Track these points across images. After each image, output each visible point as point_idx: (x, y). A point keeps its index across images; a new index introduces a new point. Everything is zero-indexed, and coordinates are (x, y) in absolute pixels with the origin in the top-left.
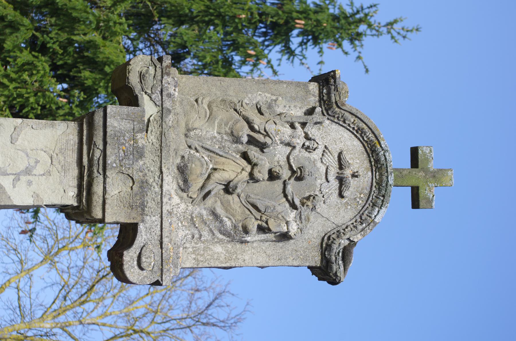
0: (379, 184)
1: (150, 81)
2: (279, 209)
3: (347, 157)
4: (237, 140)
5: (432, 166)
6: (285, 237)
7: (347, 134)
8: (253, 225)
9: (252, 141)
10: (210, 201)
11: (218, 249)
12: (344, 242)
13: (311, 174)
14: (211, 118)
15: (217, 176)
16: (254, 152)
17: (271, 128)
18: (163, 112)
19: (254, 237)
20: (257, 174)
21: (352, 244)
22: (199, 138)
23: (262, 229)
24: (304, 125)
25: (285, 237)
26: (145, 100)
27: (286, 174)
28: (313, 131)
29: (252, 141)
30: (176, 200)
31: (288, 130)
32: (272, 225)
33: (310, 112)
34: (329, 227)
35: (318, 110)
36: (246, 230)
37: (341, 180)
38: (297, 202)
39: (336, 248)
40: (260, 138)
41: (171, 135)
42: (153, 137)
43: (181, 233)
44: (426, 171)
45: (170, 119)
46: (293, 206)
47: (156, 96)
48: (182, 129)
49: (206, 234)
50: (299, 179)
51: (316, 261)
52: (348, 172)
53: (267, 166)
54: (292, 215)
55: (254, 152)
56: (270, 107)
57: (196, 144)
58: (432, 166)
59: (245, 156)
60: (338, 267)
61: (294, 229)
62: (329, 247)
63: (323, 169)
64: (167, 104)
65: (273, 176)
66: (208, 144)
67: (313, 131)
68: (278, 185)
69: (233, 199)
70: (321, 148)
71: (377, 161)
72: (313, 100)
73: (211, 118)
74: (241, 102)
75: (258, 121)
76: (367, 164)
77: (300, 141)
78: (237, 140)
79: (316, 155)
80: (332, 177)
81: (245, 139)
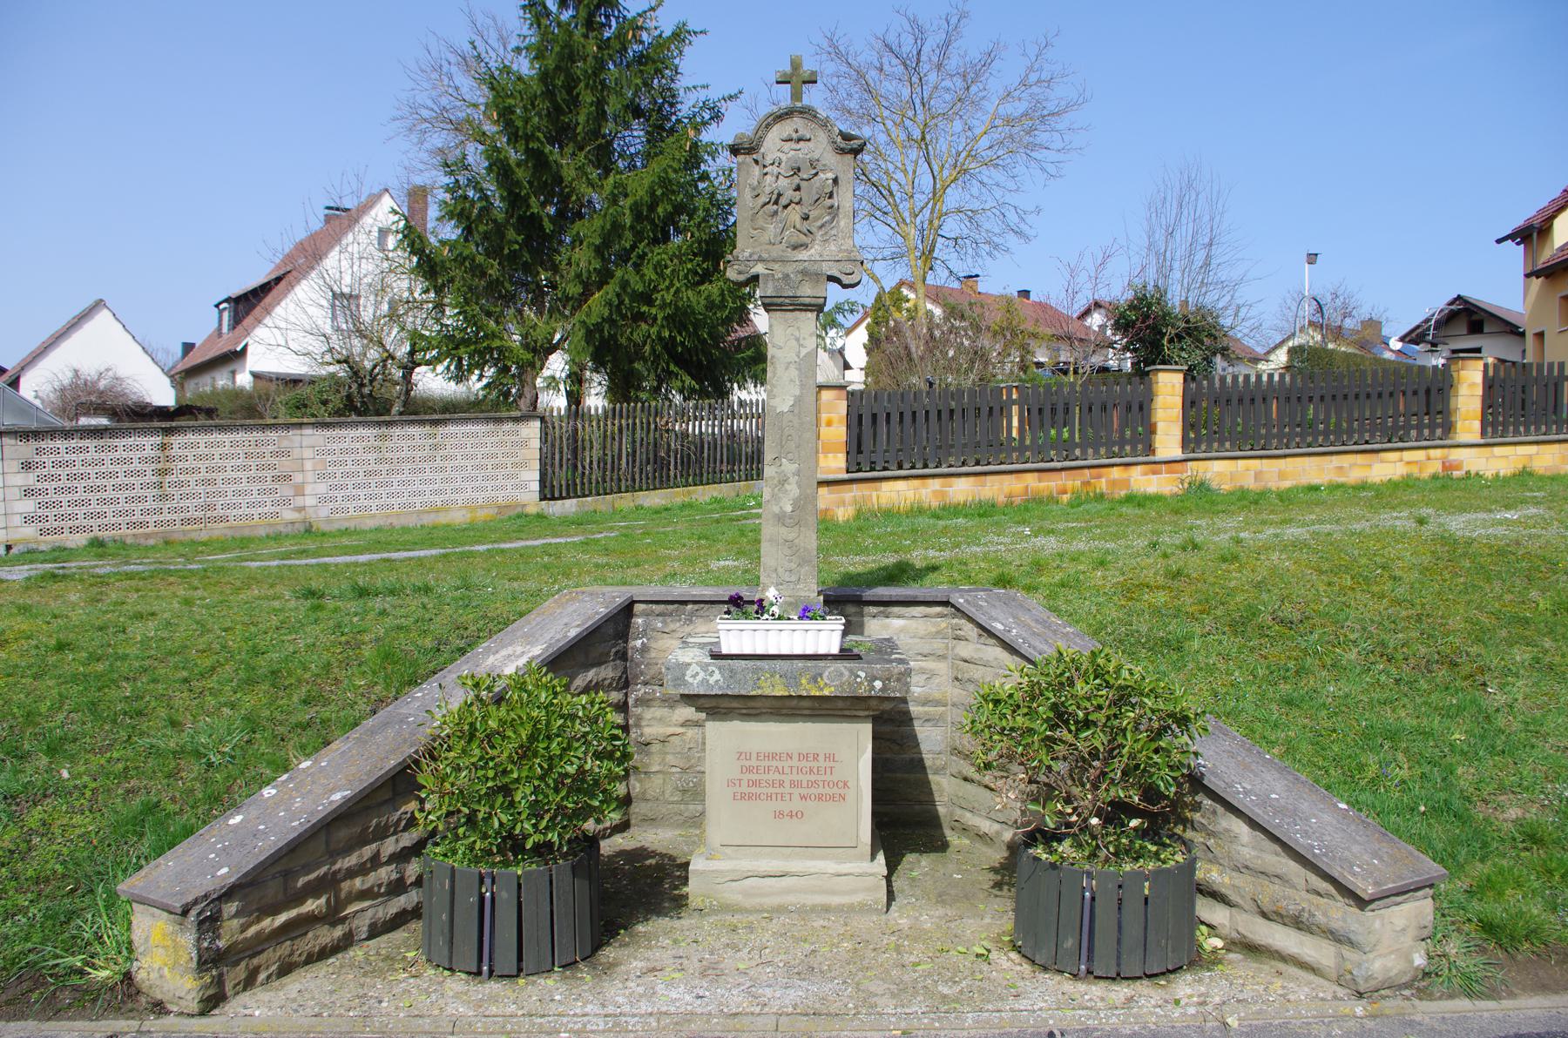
0: (801, 113)
1: (742, 268)
2: (818, 184)
3: (785, 136)
4: (776, 213)
5: (788, 69)
6: (835, 181)
7: (770, 135)
8: (828, 202)
9: (776, 203)
10: (813, 230)
11: (842, 223)
12: (839, 139)
13: (796, 162)
14: (763, 229)
15: (798, 226)
16: (783, 201)
17: (768, 190)
18: (761, 260)
19: (835, 202)
20: (796, 200)
21: (841, 133)
22: (775, 236)
23: (831, 196)
24: (765, 166)
25: (835, 181)
26: (754, 271)
27: (796, 180)
28: (768, 161)
29: (776, 203)
30: (813, 251)
31: (768, 177)
32: (828, 190)
33: (756, 162)
34: (829, 148)
35: (755, 156)
36: (831, 207)
37: (800, 140)
38: (814, 171)
39: (843, 144)
40: (774, 197)
41: (774, 254)
42: (776, 266)
43: (833, 248)
44: (792, 75)
45: (765, 256)
46: (816, 174)
47: (751, 264)
48: (770, 247)
49: (833, 232)
50: (799, 170)
51: (850, 157)
52: (795, 136)
53: (791, 192)
54: (821, 175)
55: (783, 201)
56: (754, 189)
57: (779, 239)
58: (788, 69)
59: (785, 207)
60: (855, 144)
61: (831, 175)
62: (842, 149)
63: (792, 153)
64: (756, 257)
65: (798, 189)
66: (779, 231)
67: (768, 161)
68: (803, 184)
69: (812, 215)
70: (779, 154)
71: (787, 114)
72: (749, 159)
73: (763, 229)
74: (752, 209)
75: (764, 199)
76: (788, 121)
77: (775, 169)
78: (776, 213)
79: (784, 158)
80: (798, 146)
81: (775, 207)
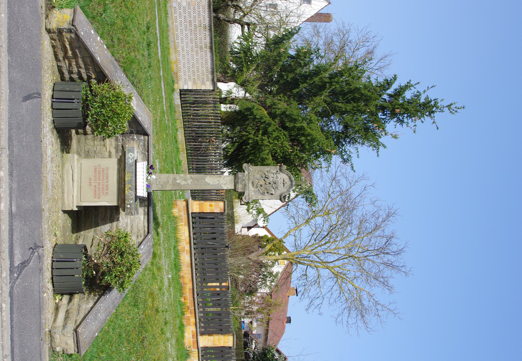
1: (247, 168)
3: (285, 180)
6: (272, 194)
7: (285, 175)
8: (266, 192)
9: (265, 177)
10: (258, 188)
11: (260, 196)
12: (284, 195)
16: (266, 179)
17: (269, 175)
18: (249, 173)
19: (266, 194)
23: (268, 193)
26: (246, 171)
28: (277, 175)
29: (265, 177)
31: (273, 175)
32: (269, 192)
33: (277, 172)
37: (284, 184)
39: (282, 196)
40: (267, 177)
41: (251, 177)
42: (247, 177)
45: (250, 174)
49: (257, 194)
52: (285, 182)
54: (273, 190)
56: (269, 171)
59: (264, 180)
61: (273, 193)
64: (250, 172)
67: (277, 175)
68: (271, 185)
69: (262, 188)
70: (279, 178)
72: (278, 169)
75: (266, 174)
77: (275, 177)
78: (262, 177)
79: (278, 179)
